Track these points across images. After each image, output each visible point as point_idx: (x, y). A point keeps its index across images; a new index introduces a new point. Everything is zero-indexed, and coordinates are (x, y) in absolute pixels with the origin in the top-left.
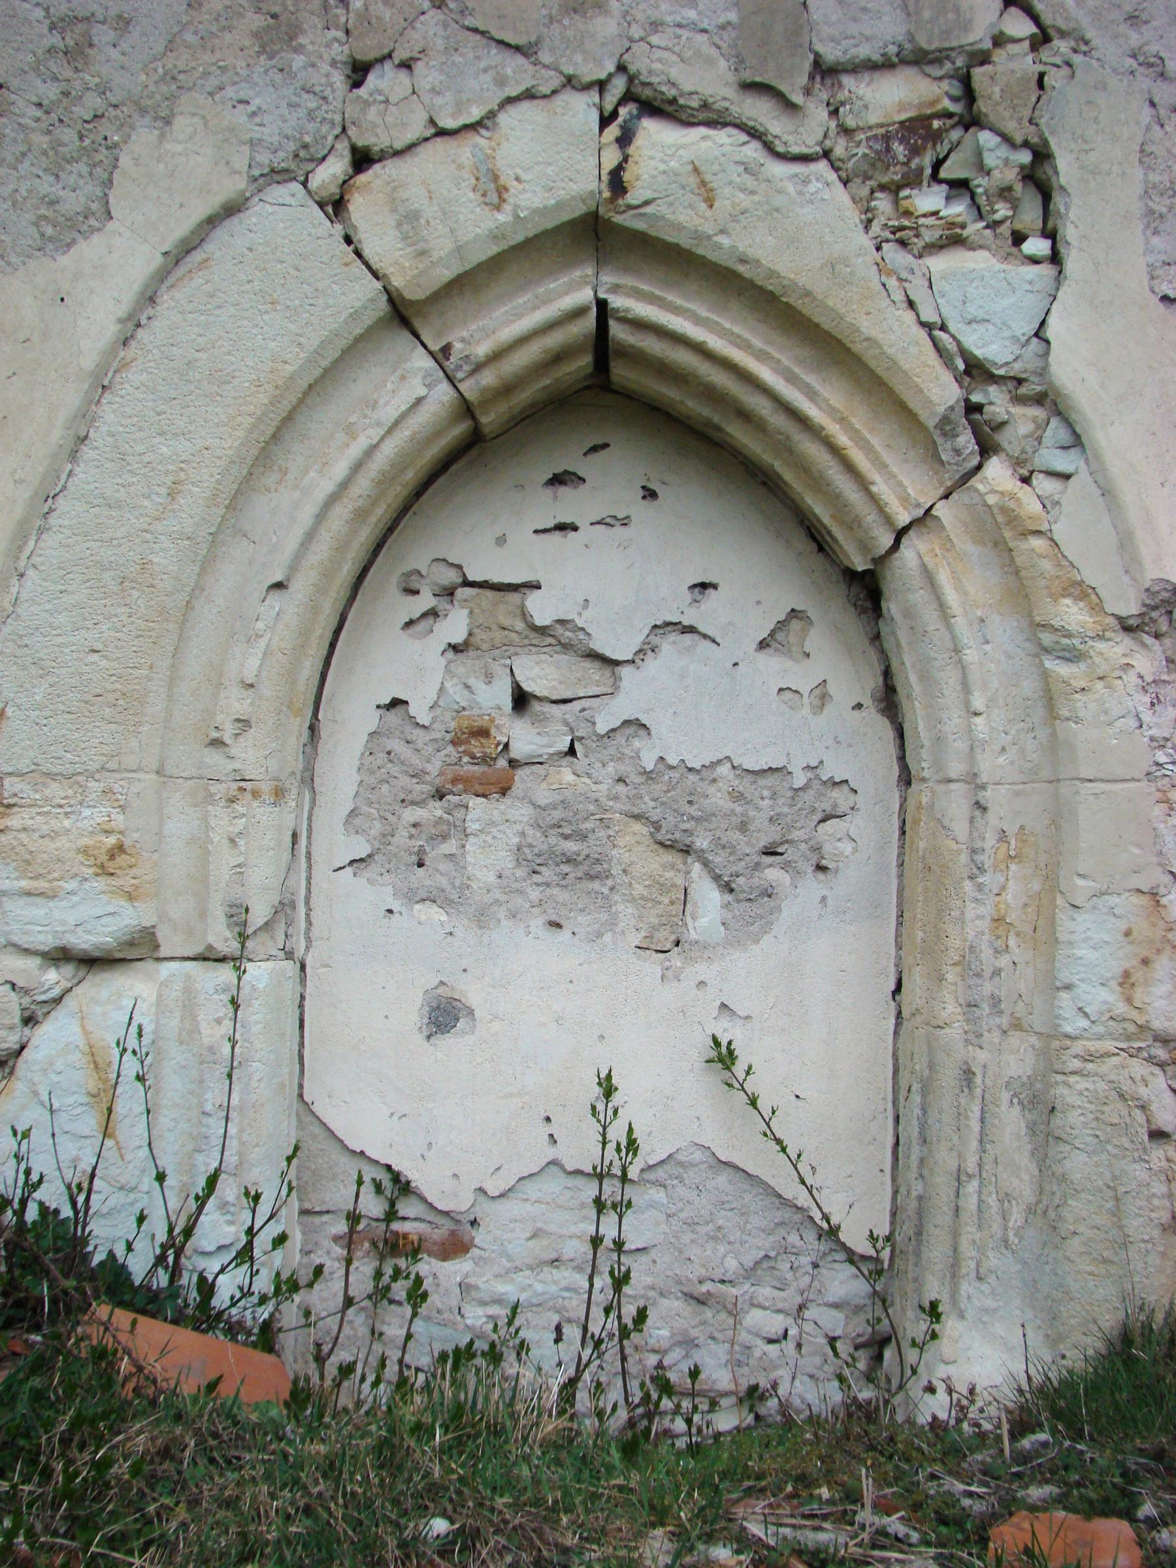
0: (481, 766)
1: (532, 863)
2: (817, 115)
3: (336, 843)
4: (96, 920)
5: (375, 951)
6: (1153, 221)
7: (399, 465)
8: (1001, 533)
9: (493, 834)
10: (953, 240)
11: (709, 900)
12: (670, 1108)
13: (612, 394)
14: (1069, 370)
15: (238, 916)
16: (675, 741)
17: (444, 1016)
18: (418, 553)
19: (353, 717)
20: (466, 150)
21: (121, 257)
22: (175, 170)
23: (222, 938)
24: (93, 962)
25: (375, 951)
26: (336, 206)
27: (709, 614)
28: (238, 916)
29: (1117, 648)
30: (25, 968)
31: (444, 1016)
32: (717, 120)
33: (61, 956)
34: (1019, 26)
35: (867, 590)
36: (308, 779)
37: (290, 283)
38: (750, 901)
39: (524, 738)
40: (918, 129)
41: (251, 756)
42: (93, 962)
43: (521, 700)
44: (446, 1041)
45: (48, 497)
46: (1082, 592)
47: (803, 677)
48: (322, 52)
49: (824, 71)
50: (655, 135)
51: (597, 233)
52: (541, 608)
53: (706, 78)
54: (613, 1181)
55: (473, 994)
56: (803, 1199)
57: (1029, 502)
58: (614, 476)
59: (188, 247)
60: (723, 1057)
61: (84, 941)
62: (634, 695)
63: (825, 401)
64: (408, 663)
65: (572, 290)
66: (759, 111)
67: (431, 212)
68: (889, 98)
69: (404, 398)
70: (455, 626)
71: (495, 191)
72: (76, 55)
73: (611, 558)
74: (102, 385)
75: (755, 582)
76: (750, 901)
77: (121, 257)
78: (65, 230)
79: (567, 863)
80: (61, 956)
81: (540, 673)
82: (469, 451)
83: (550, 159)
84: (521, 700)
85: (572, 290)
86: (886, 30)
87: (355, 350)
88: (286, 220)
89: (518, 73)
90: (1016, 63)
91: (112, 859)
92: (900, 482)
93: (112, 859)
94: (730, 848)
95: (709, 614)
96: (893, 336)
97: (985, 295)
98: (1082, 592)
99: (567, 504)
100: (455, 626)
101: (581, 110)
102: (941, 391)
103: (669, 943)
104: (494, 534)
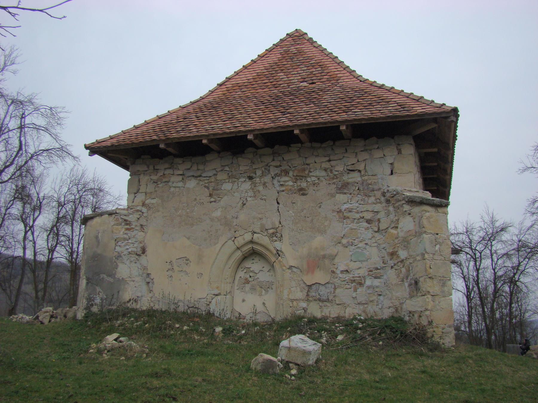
0: (247, 282)
1: (251, 289)
2: (266, 233)
3: (236, 288)
4: (216, 292)
5: (238, 296)
6: (290, 239)
7: (239, 259)
8: (280, 262)
9: (248, 287)
10: (276, 241)
11: (264, 291)
12: (260, 308)
13: (253, 253)
14: (283, 250)
15: (227, 292)
16: (261, 279)
17: (244, 301)
18: (242, 265)
19: (237, 278)
20: (242, 237)
21: (218, 246)
22: (223, 239)
23: (225, 293)
24: (217, 295)
25: (238, 296)
26: (234, 241)
27: (263, 269)
28: (227, 292)
29: (287, 270)
30: (212, 296)
31: (244, 301)
32: (259, 233)
33: (214, 295)
34: (280, 226)
35: (273, 266)
36: (233, 282)
37: (230, 246)
38: (267, 291)
39: (250, 279)
40: (273, 233)
41: (228, 280)
42: (217, 295)
43: (250, 277)
44: (244, 303)
45: (214, 262)
46: (285, 266)
47: (271, 274)
48: (233, 230)
49: (267, 230)
50: (255, 235)
51: (252, 242)
52: (251, 269)
53: (258, 230)
54: (255, 313)
55: (246, 299)
56: (267, 312)
57: (281, 260)
58: (257, 259)
59: (223, 245)
60: (264, 304)
61: (216, 293)
62: (258, 276)
63: (267, 253)
64: (241, 274)
65: (250, 246)
66: (262, 233)
67: (240, 241)
68: (271, 231)
69: (239, 254)
70: (245, 271)
71: (244, 239)
72: (217, 232)
73: (255, 265)
74: (218, 254)
75: (267, 268)
76: (267, 291)
77: (218, 246)
78: (216, 244)
79: (253, 289)
80: (214, 295)
81: (251, 274)
82: (245, 258)
83: (248, 237)
84: (250, 277)
85: (250, 246)
86: (271, 227)
87: (235, 251)
88: (230, 242)
89: (246, 231)
90: (280, 228)
91: (217, 288)
92: (273, 259)
93: (217, 288)
94: (267, 287)
95: (263, 269)
96: (271, 248)
97: (278, 245)
98: (285, 266)
99: (254, 261)
100: (245, 271)
101: (250, 233)
102: (275, 252)
103: (260, 295)
104: (248, 264)
